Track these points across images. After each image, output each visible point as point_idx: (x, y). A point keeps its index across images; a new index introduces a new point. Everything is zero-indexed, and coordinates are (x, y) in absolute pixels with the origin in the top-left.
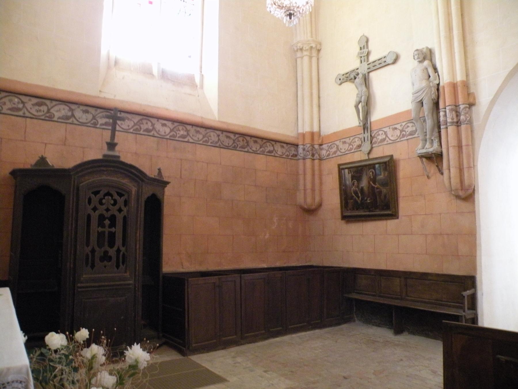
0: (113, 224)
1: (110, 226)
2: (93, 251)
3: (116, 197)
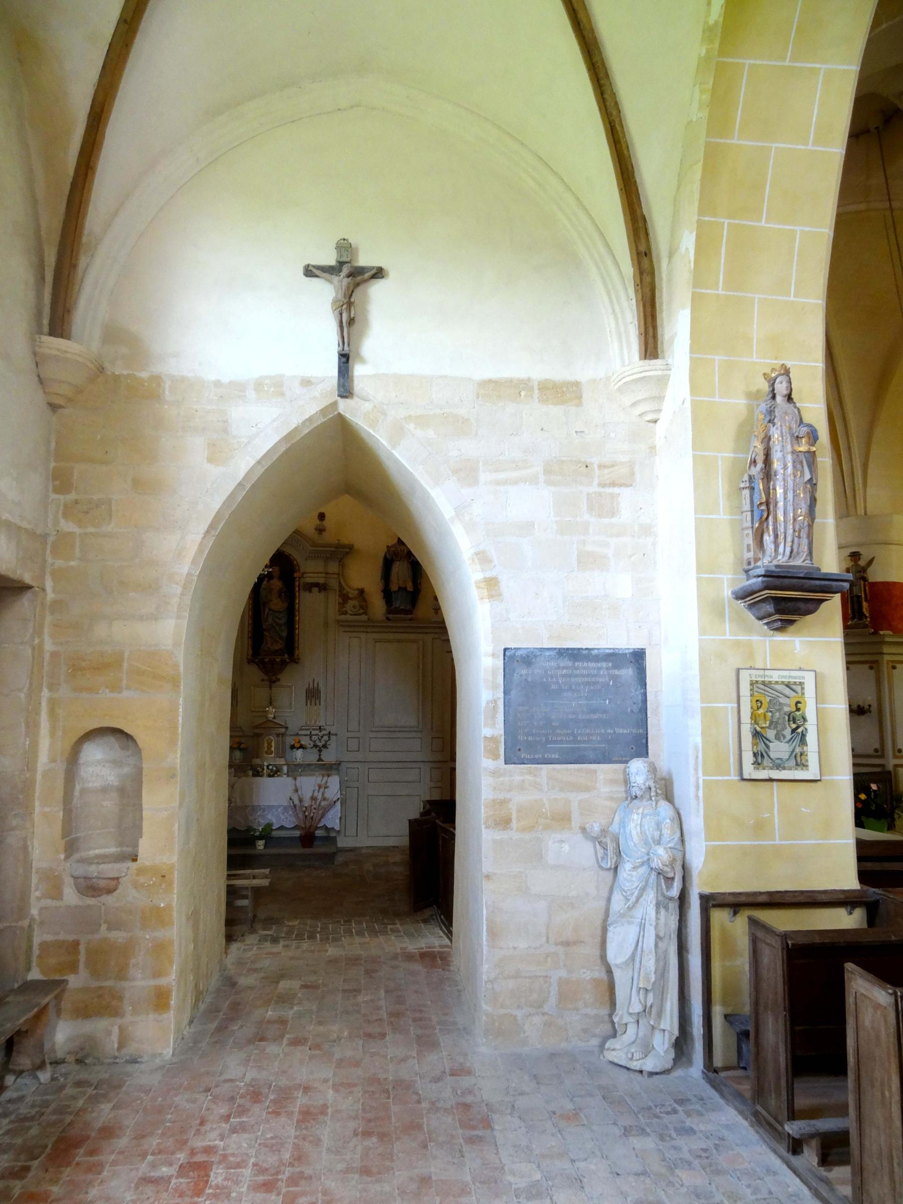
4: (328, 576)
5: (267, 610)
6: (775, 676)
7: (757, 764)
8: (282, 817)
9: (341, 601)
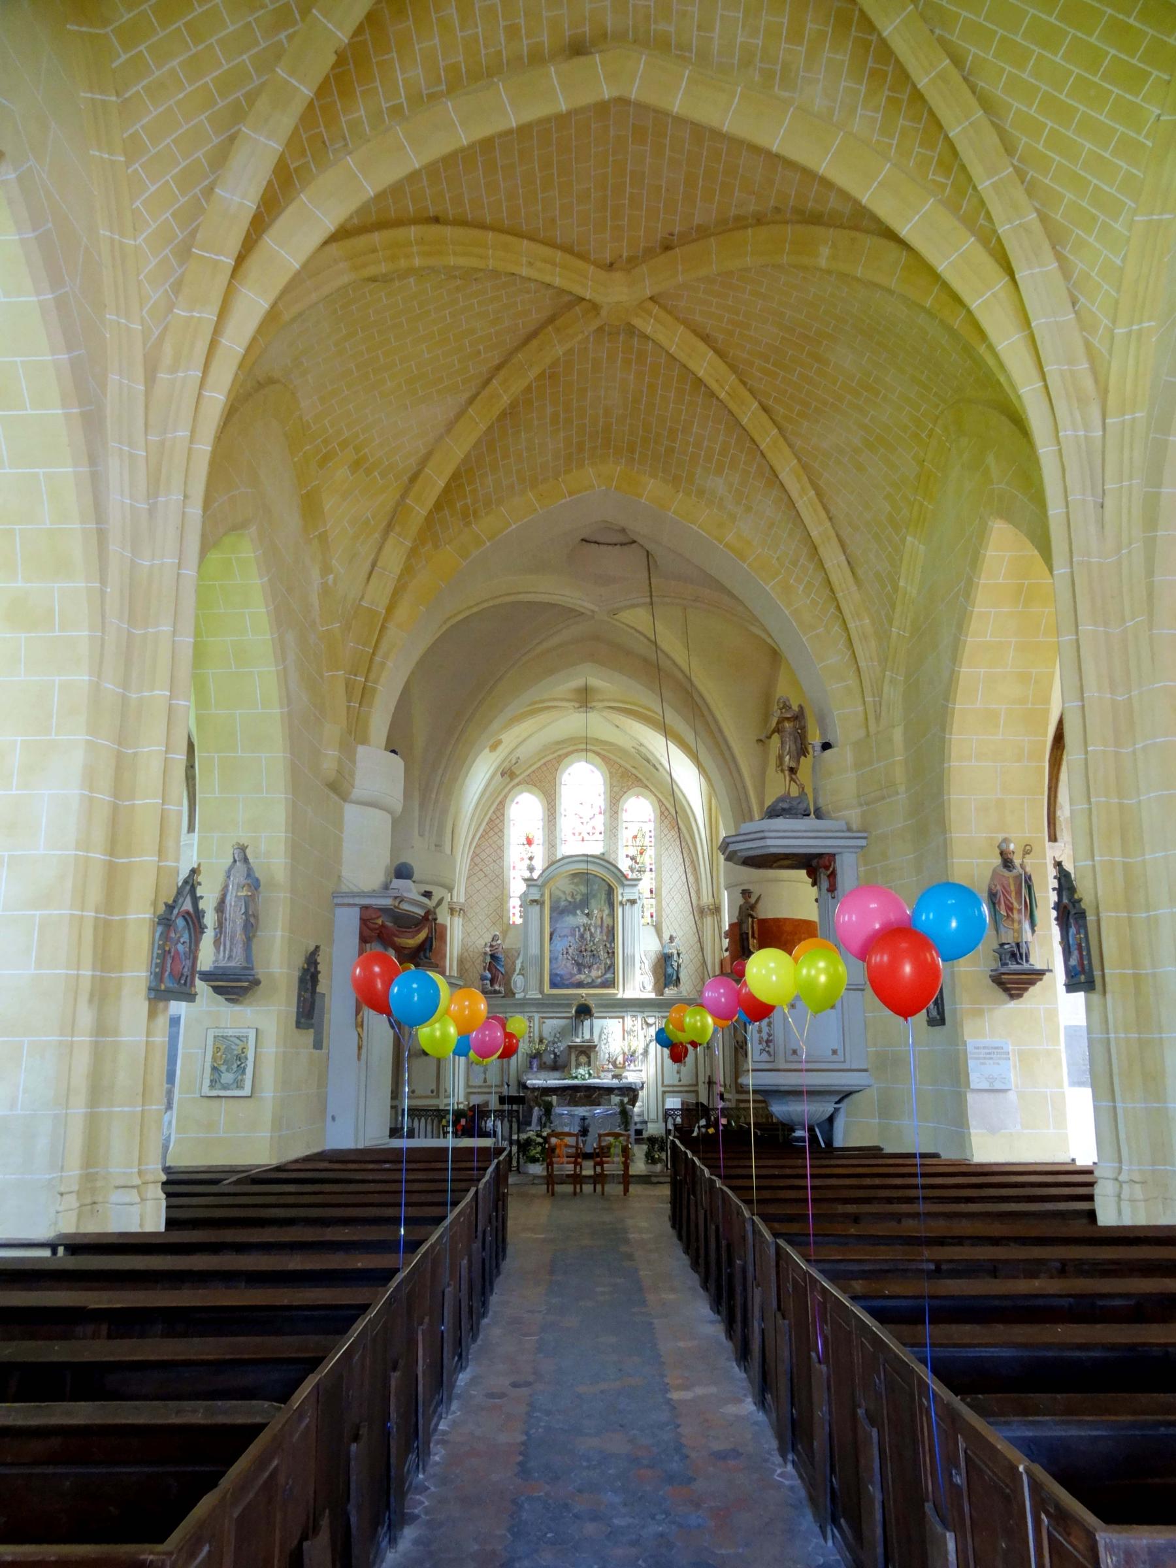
6: (230, 1032)
7: (212, 1087)
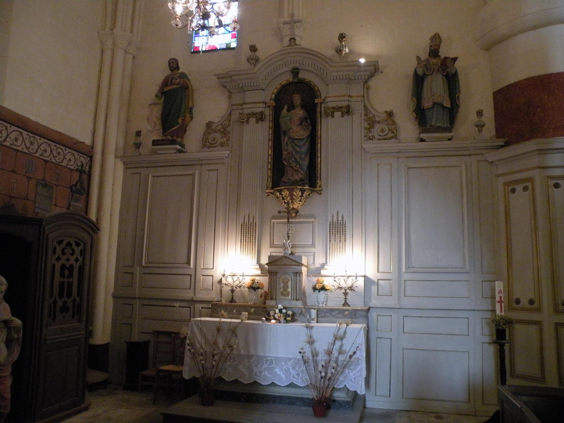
0: (71, 275)
1: (69, 277)
2: (55, 302)
3: (74, 247)
4: (352, 99)
5: (286, 139)
8: (293, 372)
9: (367, 125)
